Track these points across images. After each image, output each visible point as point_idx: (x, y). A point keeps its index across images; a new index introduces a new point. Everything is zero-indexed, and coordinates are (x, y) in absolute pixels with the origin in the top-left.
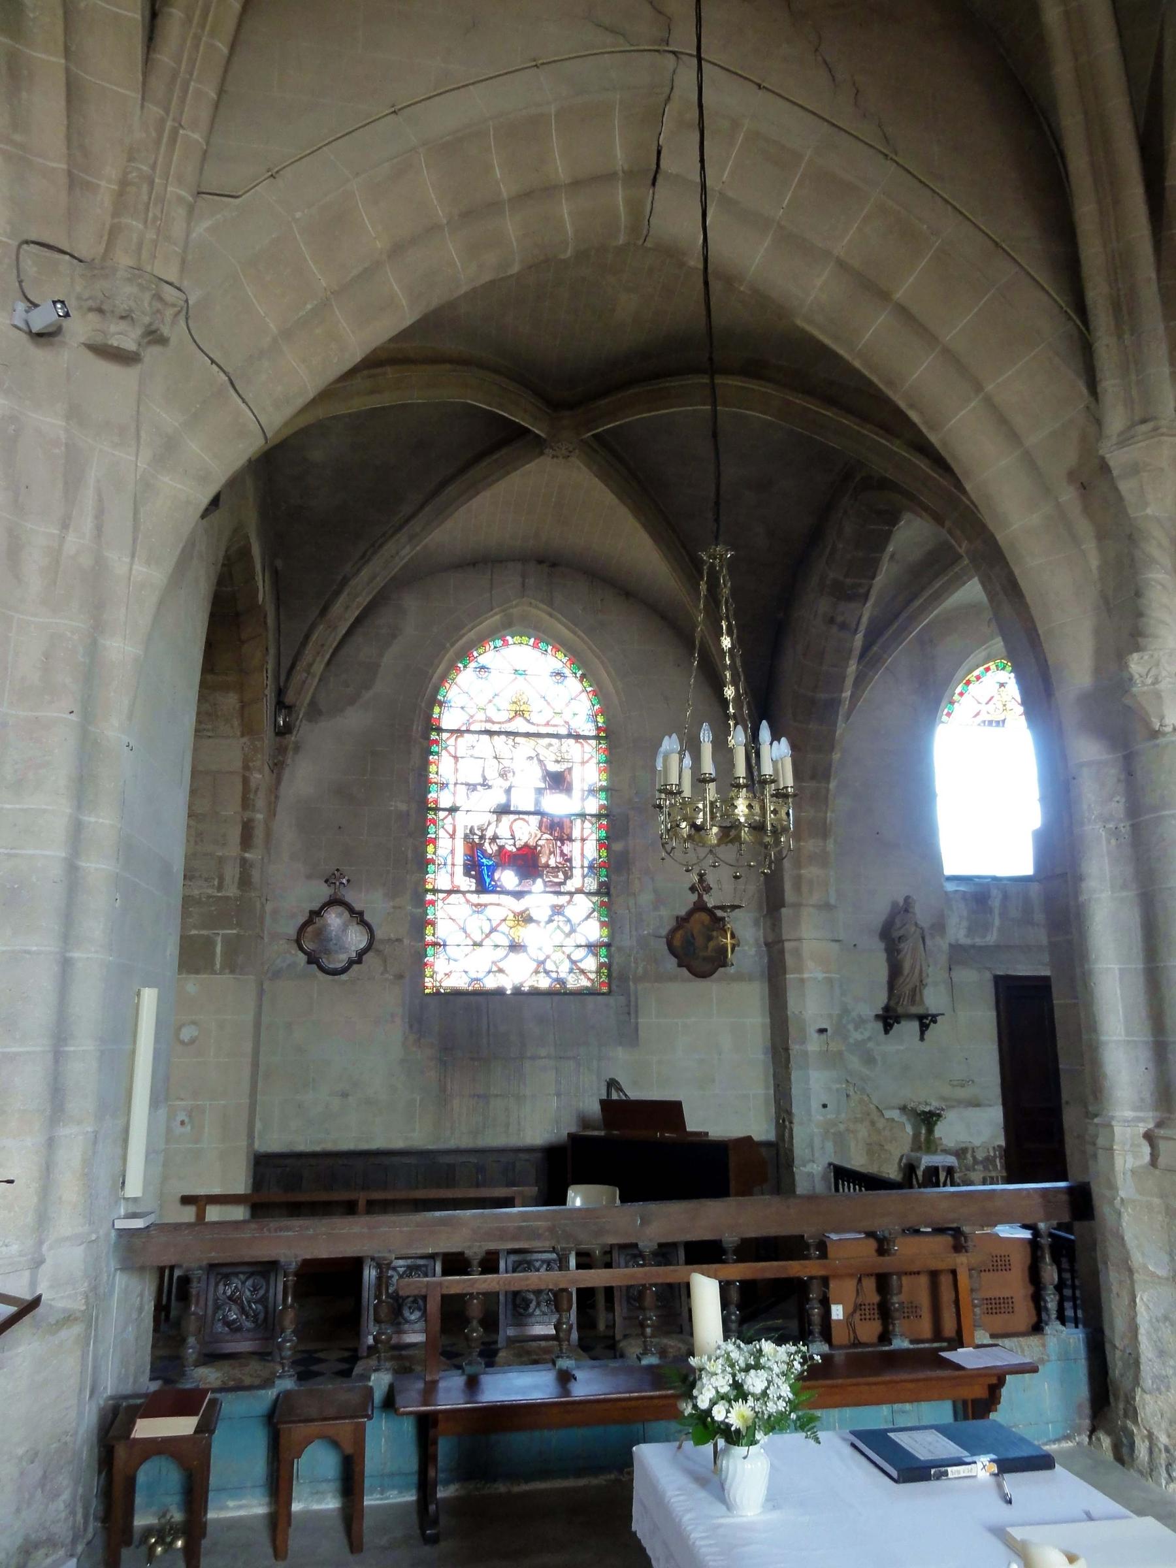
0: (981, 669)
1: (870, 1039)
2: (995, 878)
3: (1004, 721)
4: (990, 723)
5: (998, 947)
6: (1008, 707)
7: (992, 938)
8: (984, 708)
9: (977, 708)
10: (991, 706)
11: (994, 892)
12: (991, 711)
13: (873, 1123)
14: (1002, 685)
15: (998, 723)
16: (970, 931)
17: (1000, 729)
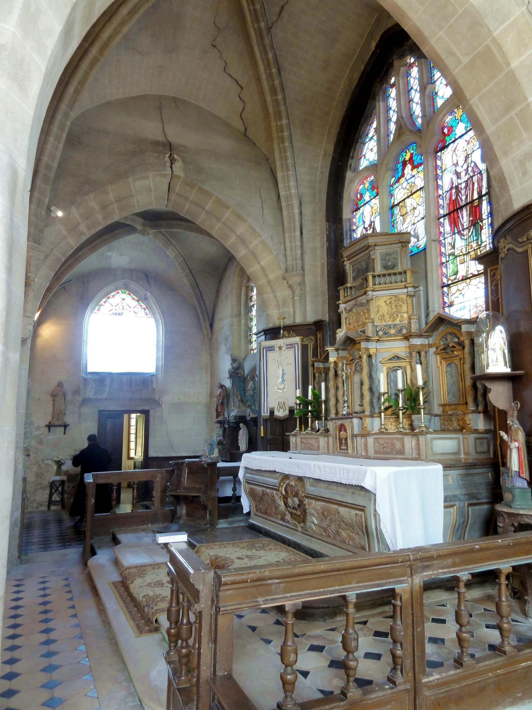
0: (115, 293)
1: (41, 434)
2: (110, 374)
3: (122, 313)
4: (116, 314)
5: (106, 399)
6: (125, 308)
7: (104, 396)
8: (114, 308)
9: (112, 308)
10: (117, 308)
11: (108, 379)
12: (117, 309)
13: (39, 465)
14: (123, 299)
15: (119, 314)
16: (95, 393)
17: (120, 317)
